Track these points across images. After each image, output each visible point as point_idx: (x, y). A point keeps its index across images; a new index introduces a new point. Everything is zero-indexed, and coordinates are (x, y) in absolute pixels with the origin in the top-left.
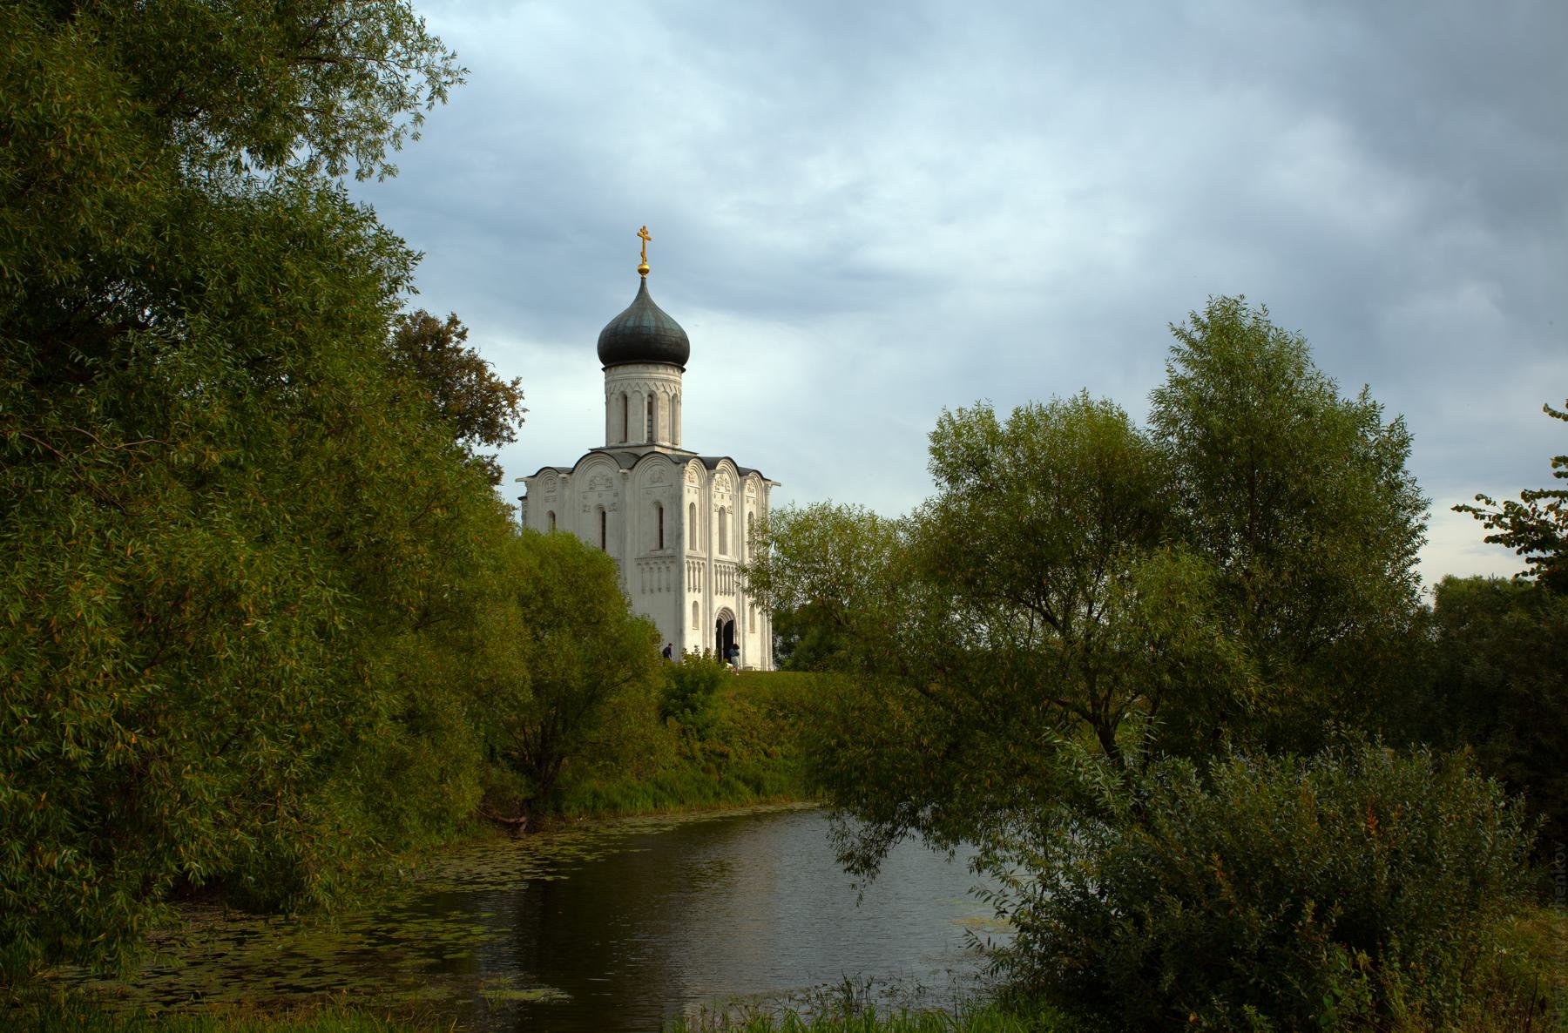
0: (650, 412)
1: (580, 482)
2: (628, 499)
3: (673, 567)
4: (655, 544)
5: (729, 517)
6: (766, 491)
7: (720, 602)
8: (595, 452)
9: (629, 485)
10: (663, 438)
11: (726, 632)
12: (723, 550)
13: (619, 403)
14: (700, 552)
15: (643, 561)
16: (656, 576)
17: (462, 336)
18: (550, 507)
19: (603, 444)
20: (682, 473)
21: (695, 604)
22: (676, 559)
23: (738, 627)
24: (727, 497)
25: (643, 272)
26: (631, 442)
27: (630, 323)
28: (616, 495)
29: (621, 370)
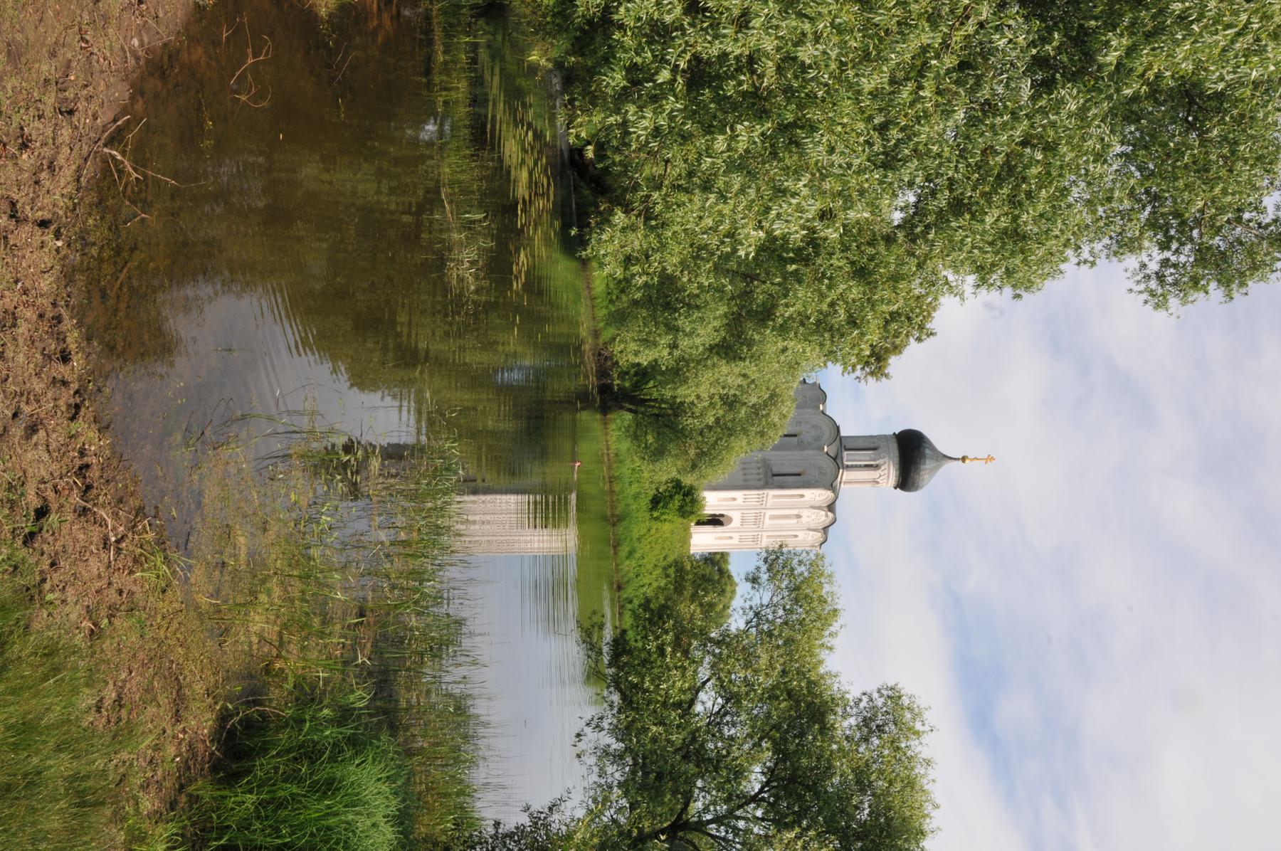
0: (866, 466)
2: (806, 452)
3: (762, 483)
4: (775, 470)
5: (795, 521)
7: (736, 516)
8: (838, 428)
9: (816, 452)
10: (846, 475)
11: (716, 521)
12: (773, 517)
13: (870, 445)
14: (771, 501)
16: (755, 471)
17: (919, 340)
19: (843, 433)
21: (734, 499)
22: (766, 485)
23: (719, 529)
25: (964, 459)
27: (927, 451)
28: (810, 444)
29: (896, 445)
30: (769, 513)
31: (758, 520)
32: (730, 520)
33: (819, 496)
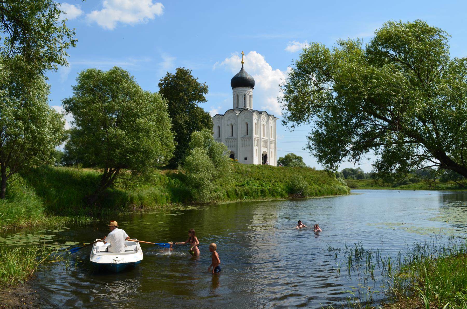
1: (226, 118)
2: (239, 122)
4: (245, 134)
5: (265, 127)
6: (275, 121)
7: (263, 150)
9: (239, 118)
10: (248, 107)
11: (265, 158)
13: (236, 98)
14: (257, 136)
15: (243, 138)
16: (246, 142)
18: (218, 125)
20: (253, 115)
21: (256, 150)
22: (251, 137)
23: (268, 156)
24: (265, 122)
26: (239, 107)
27: (239, 76)
30: (262, 137)
31: (265, 142)
32: (264, 152)
33: (255, 117)
